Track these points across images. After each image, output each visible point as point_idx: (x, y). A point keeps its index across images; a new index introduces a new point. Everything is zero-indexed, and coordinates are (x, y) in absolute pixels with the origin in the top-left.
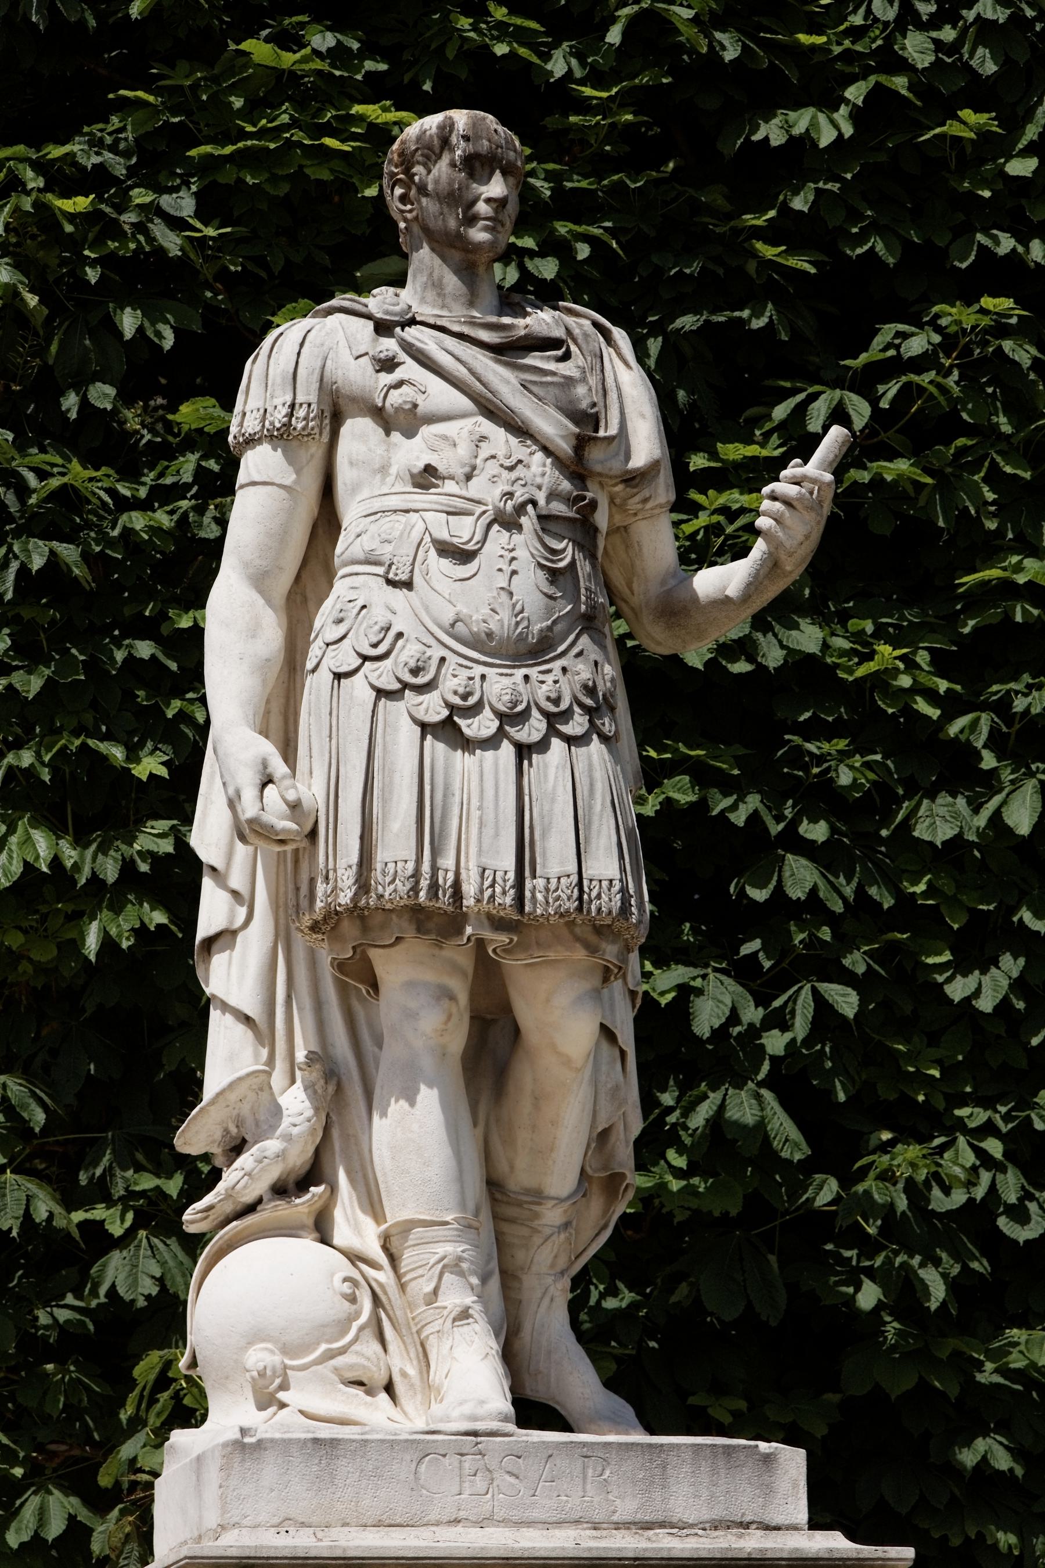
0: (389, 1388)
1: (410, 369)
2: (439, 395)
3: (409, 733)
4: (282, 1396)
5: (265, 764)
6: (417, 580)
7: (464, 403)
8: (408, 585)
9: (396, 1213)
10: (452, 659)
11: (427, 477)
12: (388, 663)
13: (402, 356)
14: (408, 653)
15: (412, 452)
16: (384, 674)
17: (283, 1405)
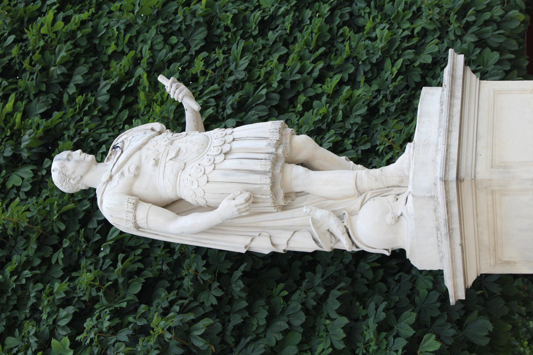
0: (398, 195)
1: (125, 169)
2: (134, 160)
3: (226, 161)
4: (399, 214)
5: (230, 199)
6: (185, 161)
7: (138, 153)
8: (185, 164)
9: (352, 190)
10: (208, 153)
11: (157, 163)
12: (206, 168)
13: (121, 171)
14: (205, 162)
15: (148, 166)
16: (209, 169)
17: (401, 215)
